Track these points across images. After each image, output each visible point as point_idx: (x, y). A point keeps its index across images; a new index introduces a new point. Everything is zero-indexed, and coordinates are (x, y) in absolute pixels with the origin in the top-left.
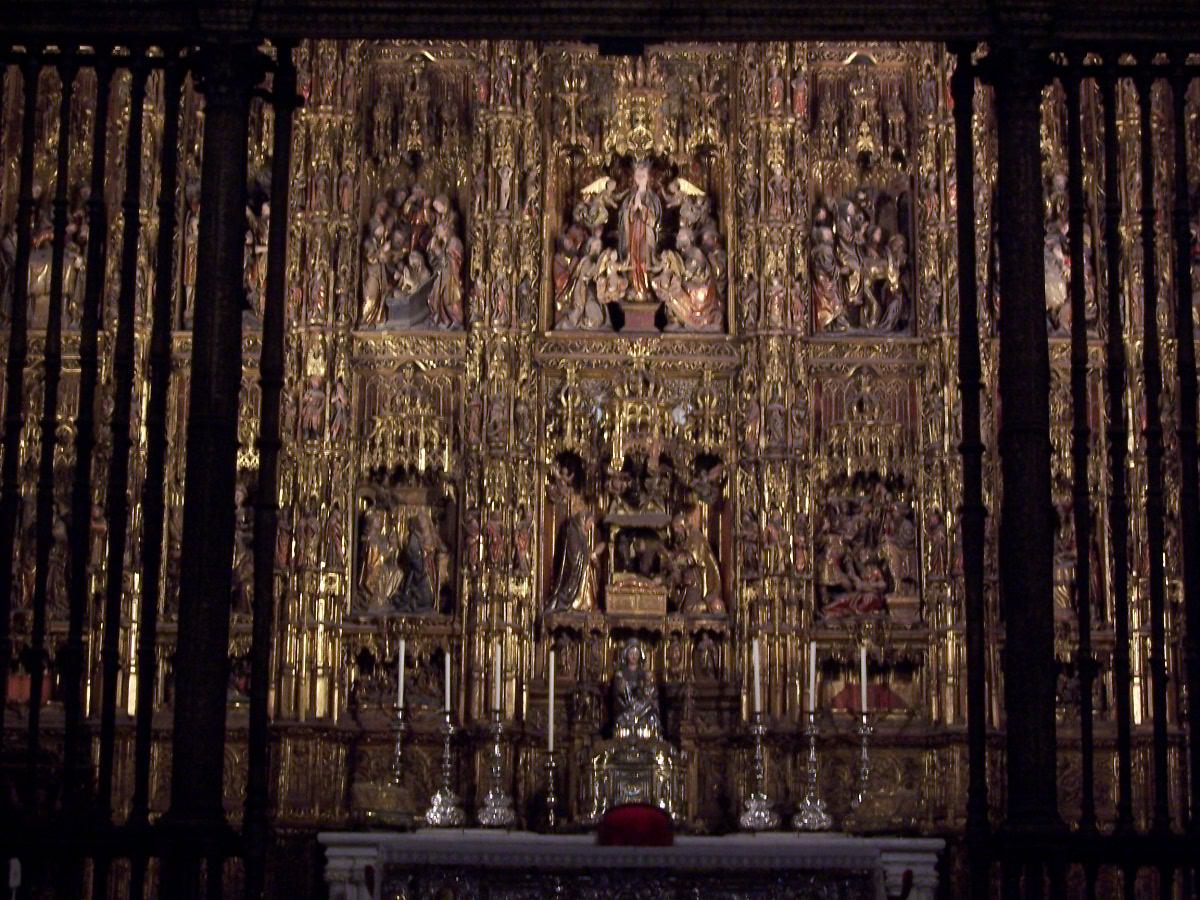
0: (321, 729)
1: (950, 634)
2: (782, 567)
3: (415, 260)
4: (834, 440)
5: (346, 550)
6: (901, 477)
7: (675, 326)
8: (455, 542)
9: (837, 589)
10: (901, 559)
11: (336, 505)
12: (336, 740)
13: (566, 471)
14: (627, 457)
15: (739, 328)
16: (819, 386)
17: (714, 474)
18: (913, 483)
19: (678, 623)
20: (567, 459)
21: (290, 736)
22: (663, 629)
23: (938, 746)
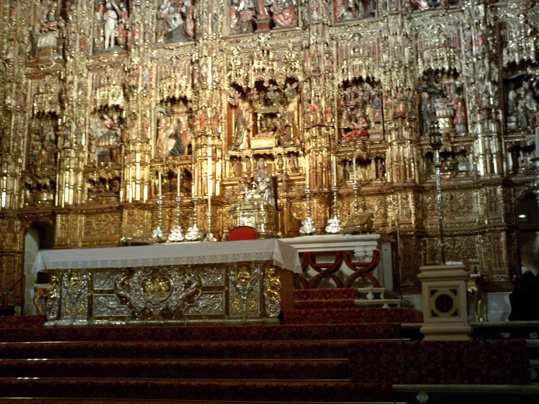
0: (138, 205)
1: (394, 143)
2: (319, 121)
3: (178, 16)
4: (344, 66)
5: (150, 133)
6: (373, 78)
7: (278, 27)
8: (191, 126)
9: (347, 130)
10: (374, 113)
11: (145, 116)
12: (146, 209)
13: (237, 92)
14: (256, 83)
15: (304, 24)
16: (337, 44)
17: (295, 85)
18: (379, 81)
19: (280, 150)
20: (235, 86)
21: (127, 209)
22: (274, 154)
23: (392, 193)
